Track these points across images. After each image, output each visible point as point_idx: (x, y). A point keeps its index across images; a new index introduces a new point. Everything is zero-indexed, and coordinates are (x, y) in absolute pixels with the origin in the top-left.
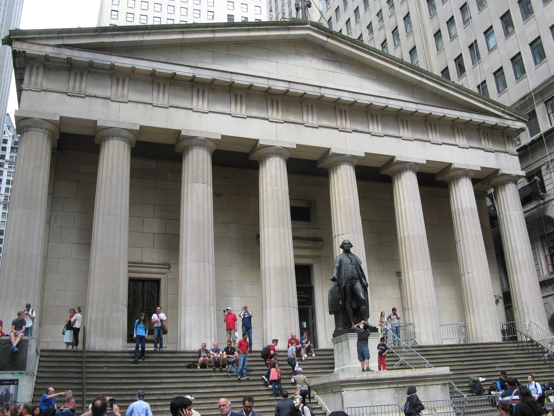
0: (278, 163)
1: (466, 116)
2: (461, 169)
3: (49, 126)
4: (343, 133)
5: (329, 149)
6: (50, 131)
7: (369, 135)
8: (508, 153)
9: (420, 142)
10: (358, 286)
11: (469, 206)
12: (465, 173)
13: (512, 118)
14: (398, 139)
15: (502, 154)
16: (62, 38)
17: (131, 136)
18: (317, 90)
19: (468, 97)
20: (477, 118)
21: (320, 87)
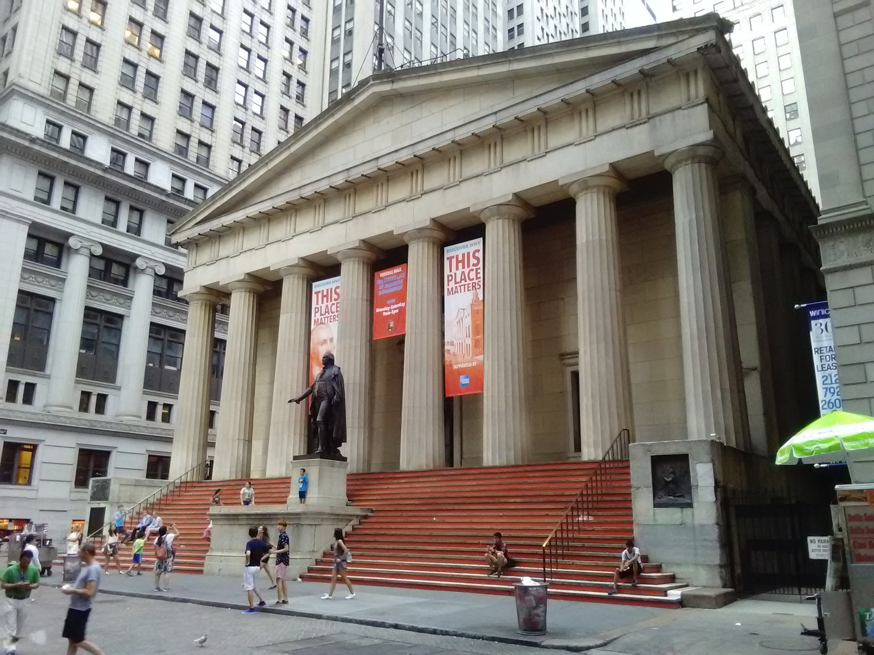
0: (351, 266)
1: (578, 88)
2: (574, 182)
3: (199, 297)
4: (411, 203)
5: (393, 231)
6: (202, 300)
7: (441, 191)
8: (680, 108)
9: (511, 167)
10: (323, 404)
11: (584, 240)
12: (585, 184)
13: (680, 39)
14: (479, 178)
15: (668, 117)
16: (195, 217)
17: (246, 285)
18: (373, 164)
19: (587, 49)
20: (598, 80)
21: (377, 158)
